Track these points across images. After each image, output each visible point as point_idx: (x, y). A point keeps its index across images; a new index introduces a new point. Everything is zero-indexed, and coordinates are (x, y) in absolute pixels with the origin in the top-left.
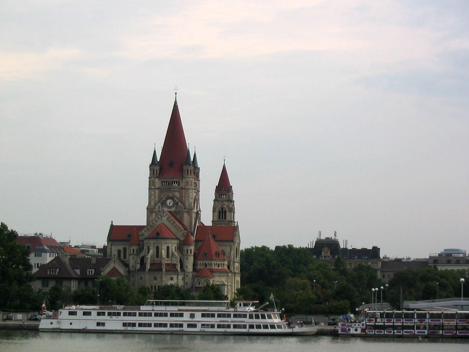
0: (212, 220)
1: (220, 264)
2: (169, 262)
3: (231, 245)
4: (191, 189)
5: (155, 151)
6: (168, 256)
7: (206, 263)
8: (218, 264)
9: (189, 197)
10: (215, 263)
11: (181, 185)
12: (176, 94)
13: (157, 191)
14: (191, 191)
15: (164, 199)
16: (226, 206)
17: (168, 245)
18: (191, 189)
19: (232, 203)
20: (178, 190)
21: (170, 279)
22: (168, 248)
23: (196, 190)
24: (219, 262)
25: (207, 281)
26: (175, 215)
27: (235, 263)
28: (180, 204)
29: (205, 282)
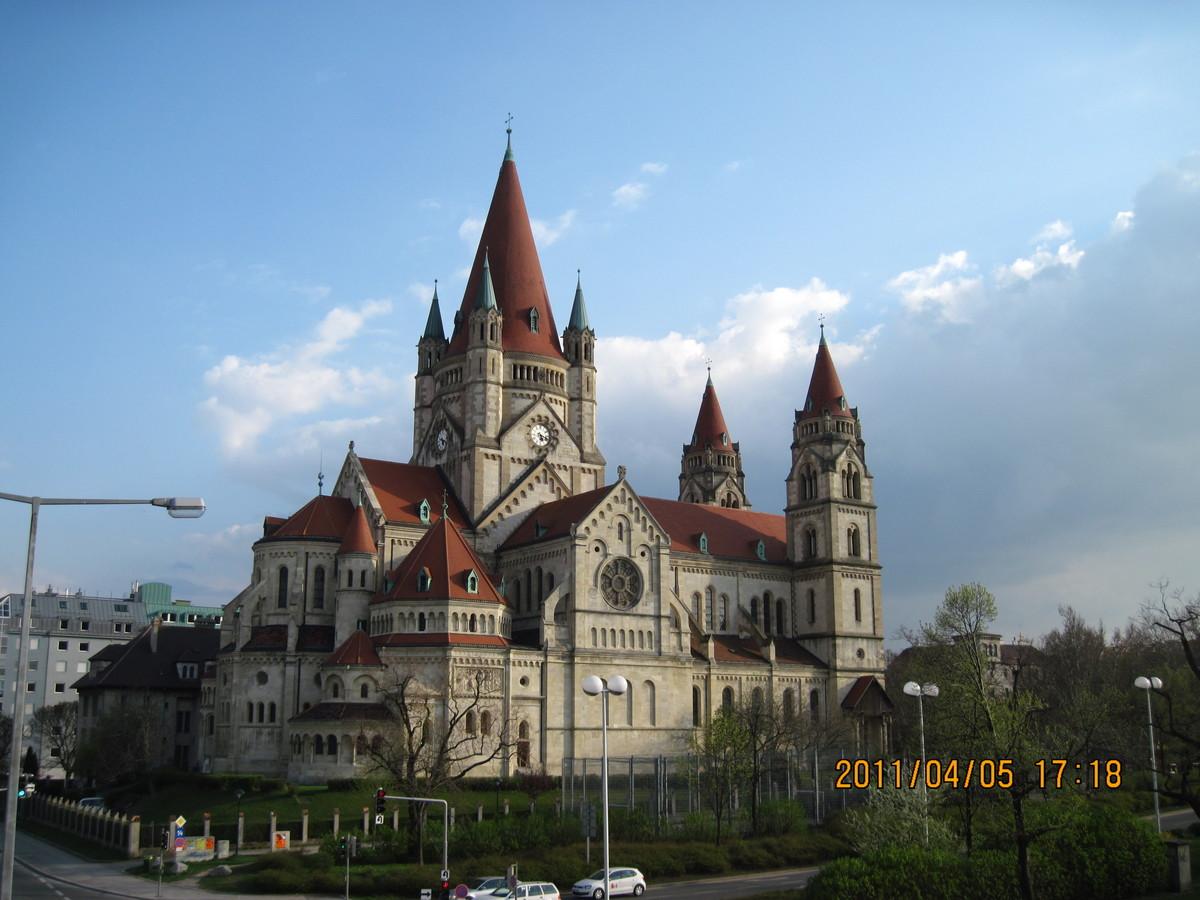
0: (785, 506)
1: (426, 616)
2: (281, 621)
3: (565, 550)
4: (480, 382)
5: (435, 302)
6: (282, 602)
7: (382, 616)
8: (417, 616)
9: (473, 406)
10: (401, 614)
11: (464, 382)
12: (509, 132)
13: (427, 415)
14: (479, 388)
15: (431, 433)
16: (816, 454)
17: (282, 561)
18: (480, 382)
19: (836, 448)
20: (456, 395)
21: (255, 679)
22: (284, 572)
23: (536, 390)
24: (422, 610)
25: (336, 681)
26: (448, 475)
27: (578, 615)
28: (456, 439)
29: (331, 685)
